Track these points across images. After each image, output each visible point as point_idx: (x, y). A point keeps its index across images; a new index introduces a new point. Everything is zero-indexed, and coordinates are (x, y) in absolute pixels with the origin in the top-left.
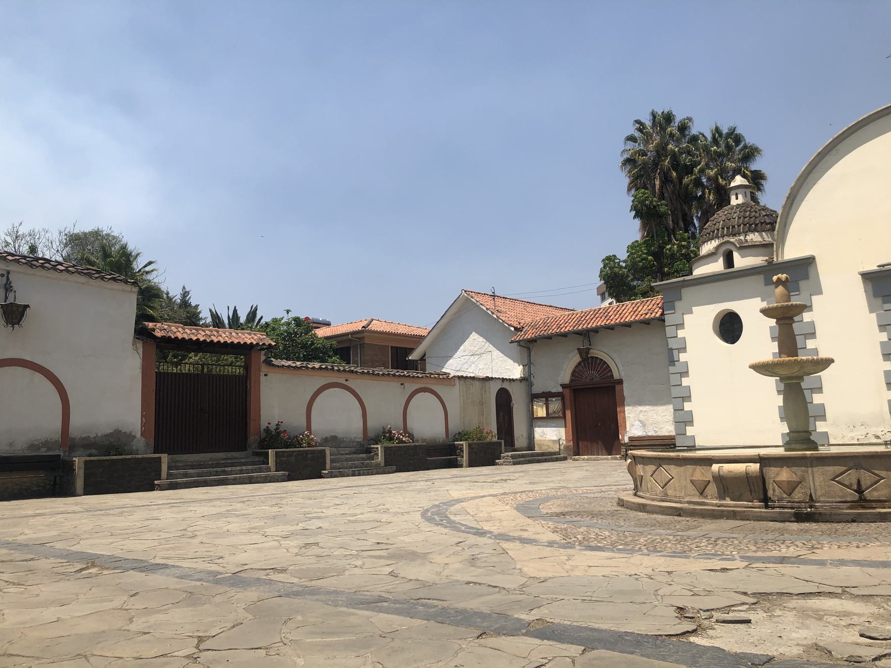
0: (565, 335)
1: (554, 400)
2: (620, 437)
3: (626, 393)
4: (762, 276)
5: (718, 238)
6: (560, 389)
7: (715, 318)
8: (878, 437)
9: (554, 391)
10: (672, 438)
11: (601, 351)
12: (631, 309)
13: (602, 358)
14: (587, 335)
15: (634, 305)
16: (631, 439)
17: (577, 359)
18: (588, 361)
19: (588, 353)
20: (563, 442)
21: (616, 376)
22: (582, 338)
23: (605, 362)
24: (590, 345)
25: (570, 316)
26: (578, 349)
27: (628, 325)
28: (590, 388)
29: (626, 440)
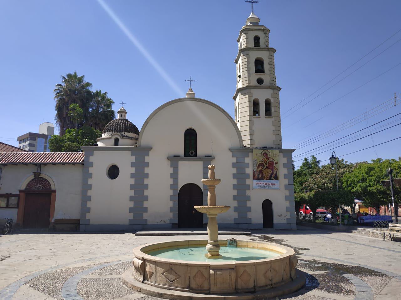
0: (26, 164)
1: (13, 198)
2: (50, 219)
3: (57, 197)
4: (130, 152)
5: (112, 131)
6: (18, 193)
7: (111, 166)
8: (164, 222)
9: (14, 193)
10: (79, 220)
11: (46, 174)
12: (66, 156)
13: (46, 179)
14: (39, 165)
15: (67, 155)
16: (56, 220)
17: (33, 177)
18: (38, 178)
19: (39, 175)
20: (15, 221)
21: (53, 188)
22: (36, 167)
23: (48, 181)
24: (41, 171)
25: (30, 154)
26: (34, 173)
27: (64, 164)
28: (37, 193)
29: (53, 221)
